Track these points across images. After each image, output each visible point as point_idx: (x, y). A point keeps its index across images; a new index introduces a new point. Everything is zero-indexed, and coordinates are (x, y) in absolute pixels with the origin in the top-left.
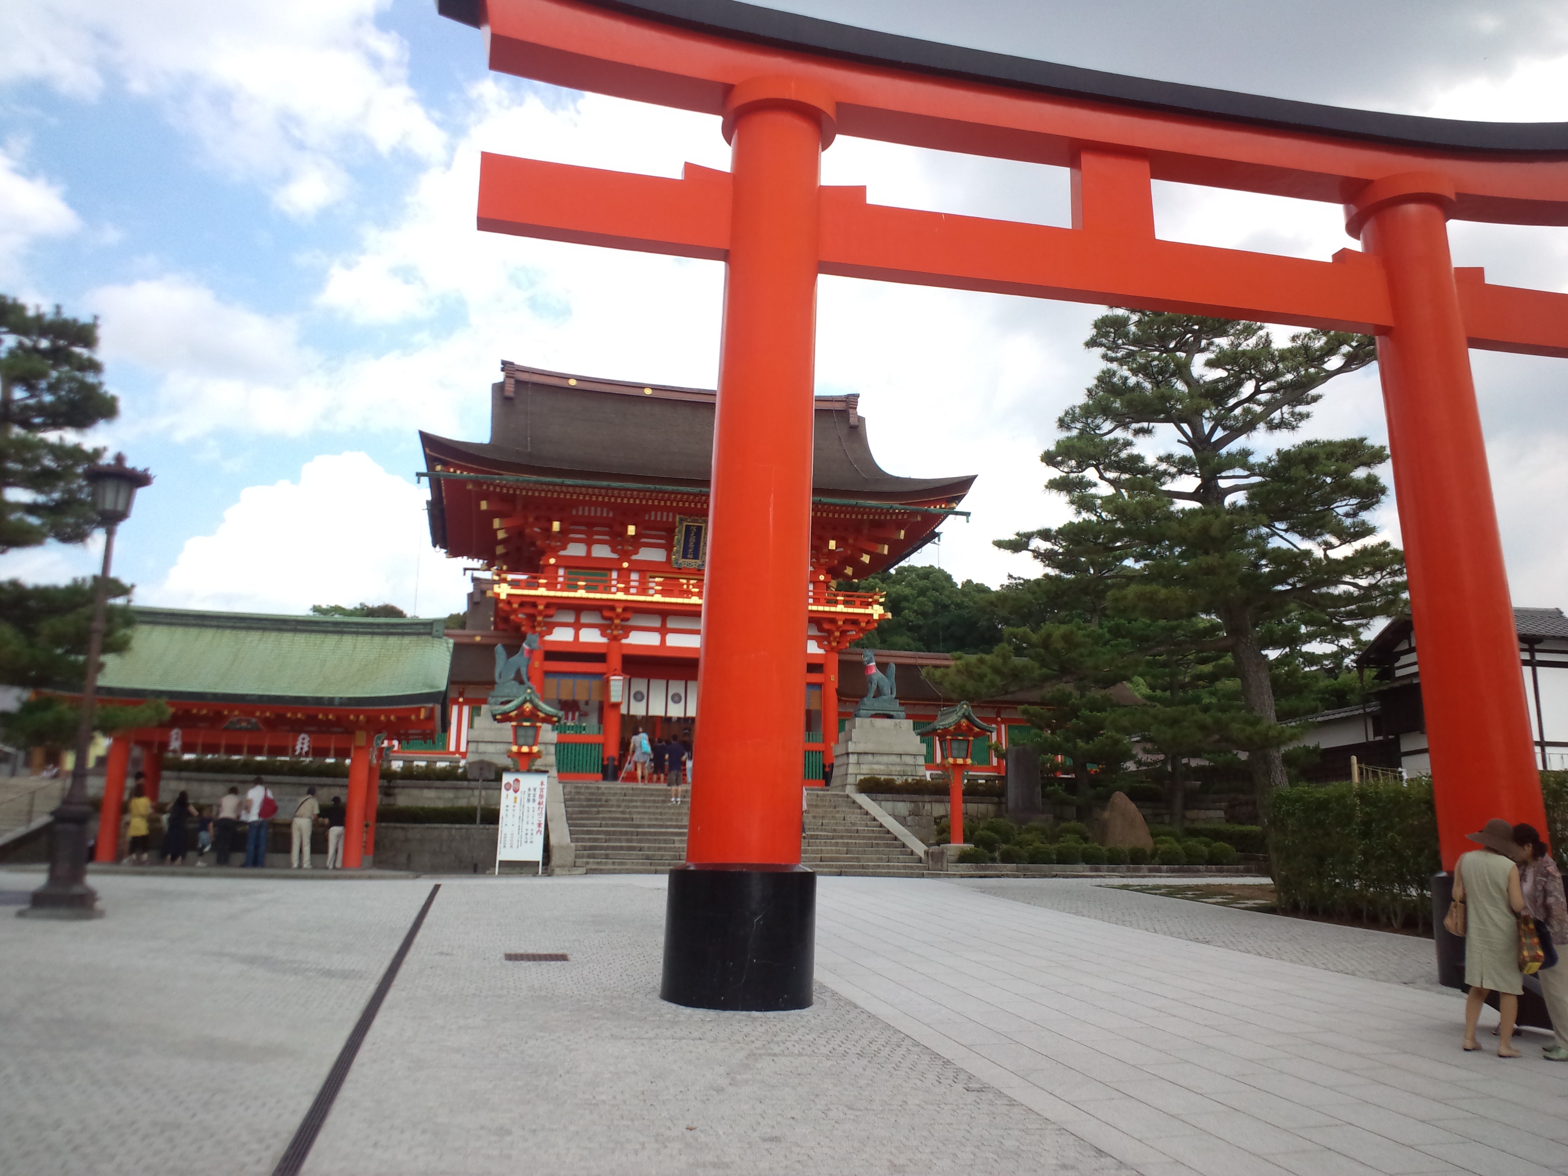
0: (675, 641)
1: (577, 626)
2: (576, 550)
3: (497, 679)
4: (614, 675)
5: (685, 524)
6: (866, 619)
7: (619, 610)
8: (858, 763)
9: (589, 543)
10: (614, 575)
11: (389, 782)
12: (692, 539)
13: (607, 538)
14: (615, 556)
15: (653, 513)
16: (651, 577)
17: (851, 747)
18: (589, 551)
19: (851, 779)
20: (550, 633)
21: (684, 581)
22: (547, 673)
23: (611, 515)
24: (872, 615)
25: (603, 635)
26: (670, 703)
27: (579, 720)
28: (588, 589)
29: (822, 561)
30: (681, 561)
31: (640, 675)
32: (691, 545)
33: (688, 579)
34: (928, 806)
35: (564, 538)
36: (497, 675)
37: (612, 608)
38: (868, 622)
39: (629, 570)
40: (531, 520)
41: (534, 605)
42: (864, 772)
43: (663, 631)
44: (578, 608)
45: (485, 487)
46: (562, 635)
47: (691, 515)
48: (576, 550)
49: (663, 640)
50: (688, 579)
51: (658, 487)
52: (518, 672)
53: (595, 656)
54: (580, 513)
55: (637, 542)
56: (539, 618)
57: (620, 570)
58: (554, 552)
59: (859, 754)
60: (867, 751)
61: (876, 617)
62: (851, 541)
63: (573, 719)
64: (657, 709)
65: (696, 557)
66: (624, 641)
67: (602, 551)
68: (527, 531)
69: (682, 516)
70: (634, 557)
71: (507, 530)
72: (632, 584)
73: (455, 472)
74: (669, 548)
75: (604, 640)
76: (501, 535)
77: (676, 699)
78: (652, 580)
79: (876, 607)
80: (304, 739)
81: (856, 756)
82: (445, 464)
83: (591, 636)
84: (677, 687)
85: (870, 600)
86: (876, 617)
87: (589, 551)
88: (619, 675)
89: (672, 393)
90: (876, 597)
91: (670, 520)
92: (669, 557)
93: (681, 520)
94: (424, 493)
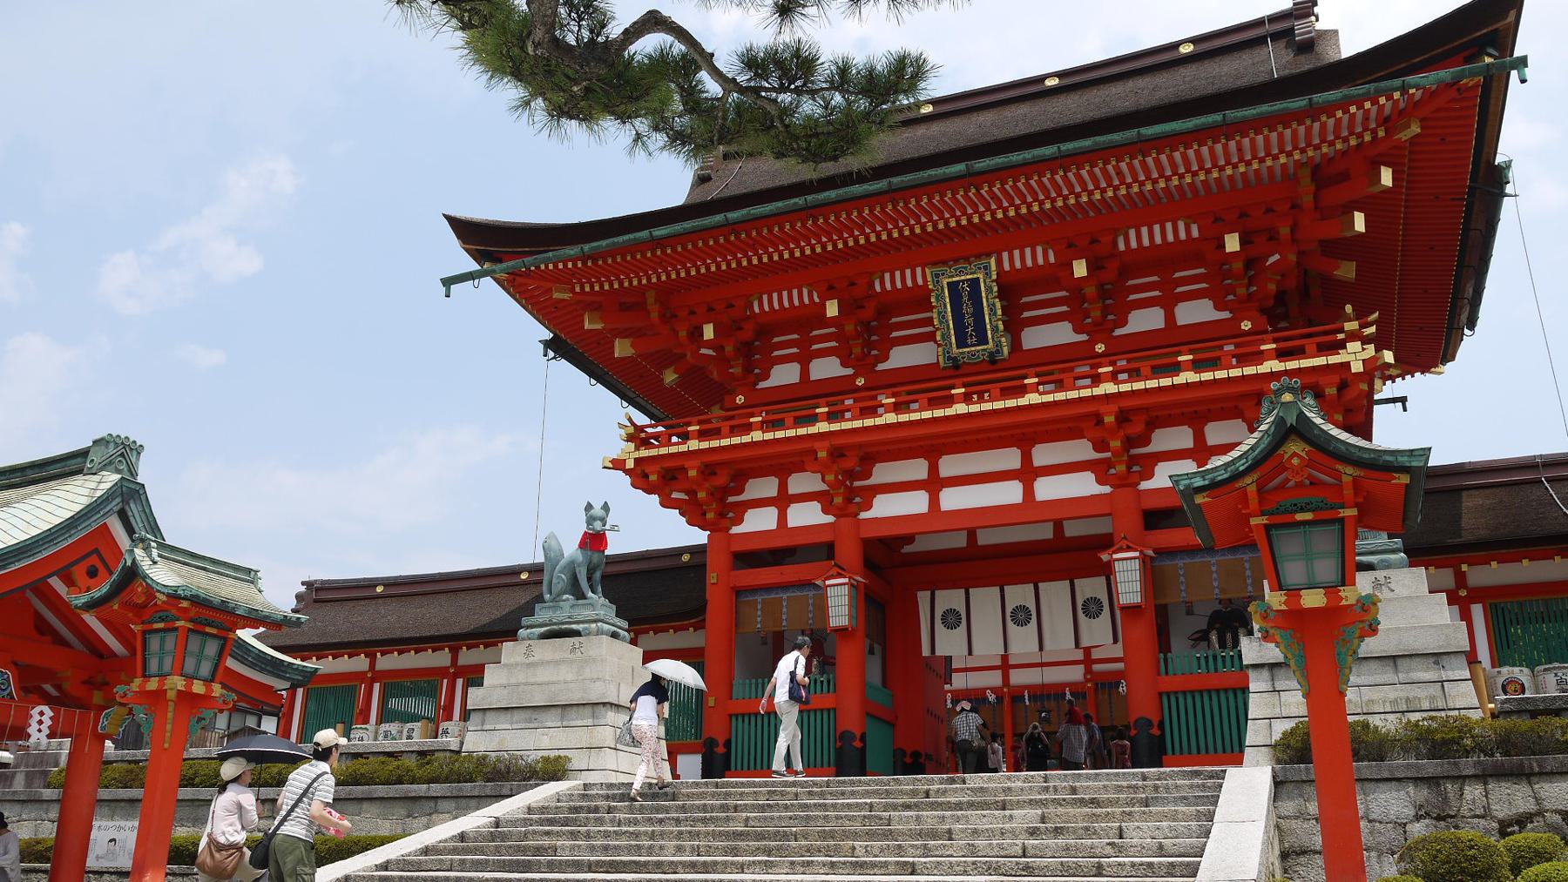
0: (953, 499)
6: (1336, 378)
12: (968, 309)
13: (834, 344)
14: (849, 371)
15: (887, 276)
18: (805, 372)
19: (1255, 734)
20: (739, 521)
22: (738, 592)
24: (1347, 365)
29: (1242, 291)
31: (954, 585)
32: (969, 320)
34: (1473, 792)
38: (1342, 387)
40: (683, 334)
43: (934, 484)
45: (578, 289)
46: (760, 521)
47: (956, 261)
48: (785, 375)
49: (934, 502)
51: (810, 198)
56: (701, 495)
58: (749, 386)
61: (1357, 367)
62: (1285, 231)
66: (864, 515)
67: (826, 368)
75: (830, 519)
77: (1021, 616)
79: (1353, 346)
80: (42, 714)
81: (1265, 673)
82: (495, 258)
83: (807, 515)
84: (1020, 594)
85: (1341, 336)
86: (1357, 367)
88: (839, 576)
89: (986, 118)
90: (1352, 326)
91: (920, 282)
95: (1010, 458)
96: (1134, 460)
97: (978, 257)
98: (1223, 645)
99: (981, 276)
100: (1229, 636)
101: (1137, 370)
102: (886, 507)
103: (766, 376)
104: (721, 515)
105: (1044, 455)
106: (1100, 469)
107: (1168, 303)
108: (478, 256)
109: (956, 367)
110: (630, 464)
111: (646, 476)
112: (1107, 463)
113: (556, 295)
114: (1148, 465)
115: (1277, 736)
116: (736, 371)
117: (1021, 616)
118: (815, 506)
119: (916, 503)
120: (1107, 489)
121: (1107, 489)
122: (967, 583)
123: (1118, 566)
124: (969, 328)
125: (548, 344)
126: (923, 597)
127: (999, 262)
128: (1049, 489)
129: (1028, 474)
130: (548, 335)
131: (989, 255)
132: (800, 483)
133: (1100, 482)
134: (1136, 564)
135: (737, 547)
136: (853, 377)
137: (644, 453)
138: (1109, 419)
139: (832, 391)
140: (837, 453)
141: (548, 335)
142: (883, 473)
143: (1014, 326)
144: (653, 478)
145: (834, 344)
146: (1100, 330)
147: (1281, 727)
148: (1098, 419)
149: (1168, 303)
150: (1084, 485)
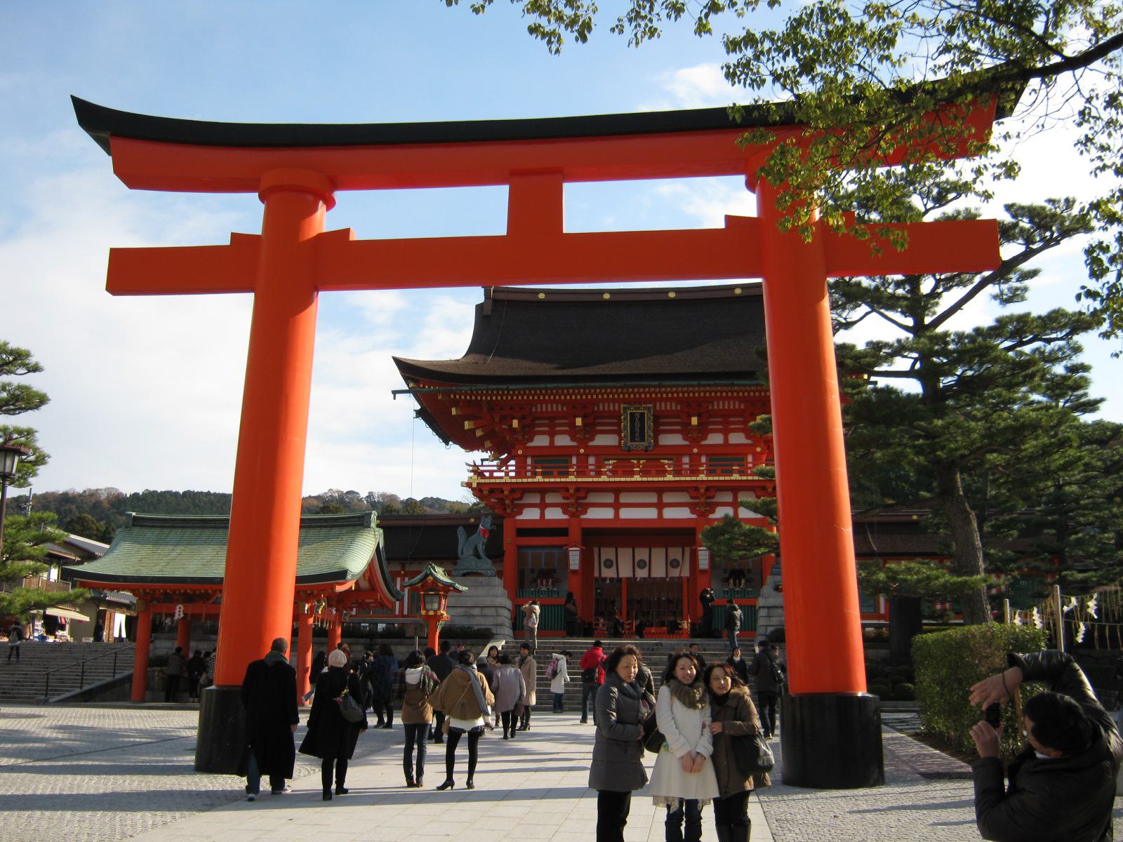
0: (626, 514)
1: (543, 506)
2: (541, 441)
3: (460, 555)
4: (572, 546)
5: (629, 412)
7: (572, 491)
8: (769, 616)
9: (552, 434)
10: (574, 460)
11: (371, 640)
12: (638, 425)
14: (574, 444)
16: (605, 460)
17: (760, 602)
20: (521, 513)
21: (635, 462)
22: (519, 547)
23: (565, 409)
25: (564, 512)
26: (670, 568)
27: (553, 586)
28: (544, 474)
30: (630, 444)
32: (637, 430)
33: (639, 460)
35: (529, 430)
36: (459, 552)
37: (567, 490)
39: (587, 455)
40: (497, 419)
41: (502, 491)
42: (774, 623)
43: (617, 506)
44: (543, 490)
46: (531, 514)
48: (541, 441)
49: (617, 514)
50: (639, 460)
52: (476, 549)
53: (558, 531)
54: (539, 409)
55: (590, 429)
56: (507, 502)
57: (578, 455)
58: (522, 444)
59: (769, 608)
60: (776, 604)
63: (547, 584)
64: (625, 572)
65: (643, 439)
66: (583, 517)
67: (563, 441)
68: (497, 429)
69: (625, 406)
70: (591, 444)
71: (483, 427)
72: (590, 467)
73: (424, 387)
74: (618, 432)
75: (566, 517)
76: (479, 433)
77: (642, 564)
78: (606, 462)
81: (766, 610)
83: (555, 514)
84: (642, 554)
87: (552, 441)
88: (576, 546)
91: (617, 408)
92: (620, 442)
93: (625, 409)
94: (410, 404)
95: (653, 498)
96: (709, 504)
97: (645, 403)
98: (735, 584)
99: (646, 412)
100: (737, 581)
101: (715, 471)
102: (594, 514)
103: (532, 440)
104: (512, 510)
105: (667, 498)
106: (693, 508)
107: (726, 432)
108: (407, 379)
109: (629, 451)
110: (475, 485)
111: (481, 490)
112: (696, 505)
113: (440, 397)
114: (712, 507)
115: (768, 633)
116: (520, 438)
117: (642, 564)
118: (559, 510)
119: (608, 514)
120: (694, 516)
121: (694, 516)
122: (616, 546)
123: (700, 553)
124: (637, 433)
125: (419, 414)
126: (596, 550)
127: (655, 406)
128: (669, 513)
129: (660, 506)
130: (418, 407)
131: (650, 403)
132: (550, 499)
133: (692, 512)
134: (707, 552)
135: (520, 526)
136: (578, 448)
137: (483, 481)
138: (702, 491)
139: (565, 453)
140: (577, 490)
141: (418, 407)
142: (592, 498)
143: (657, 433)
144: (485, 493)
145: (566, 428)
146: (695, 441)
147: (770, 629)
148: (697, 489)
149: (726, 432)
150: (684, 514)
